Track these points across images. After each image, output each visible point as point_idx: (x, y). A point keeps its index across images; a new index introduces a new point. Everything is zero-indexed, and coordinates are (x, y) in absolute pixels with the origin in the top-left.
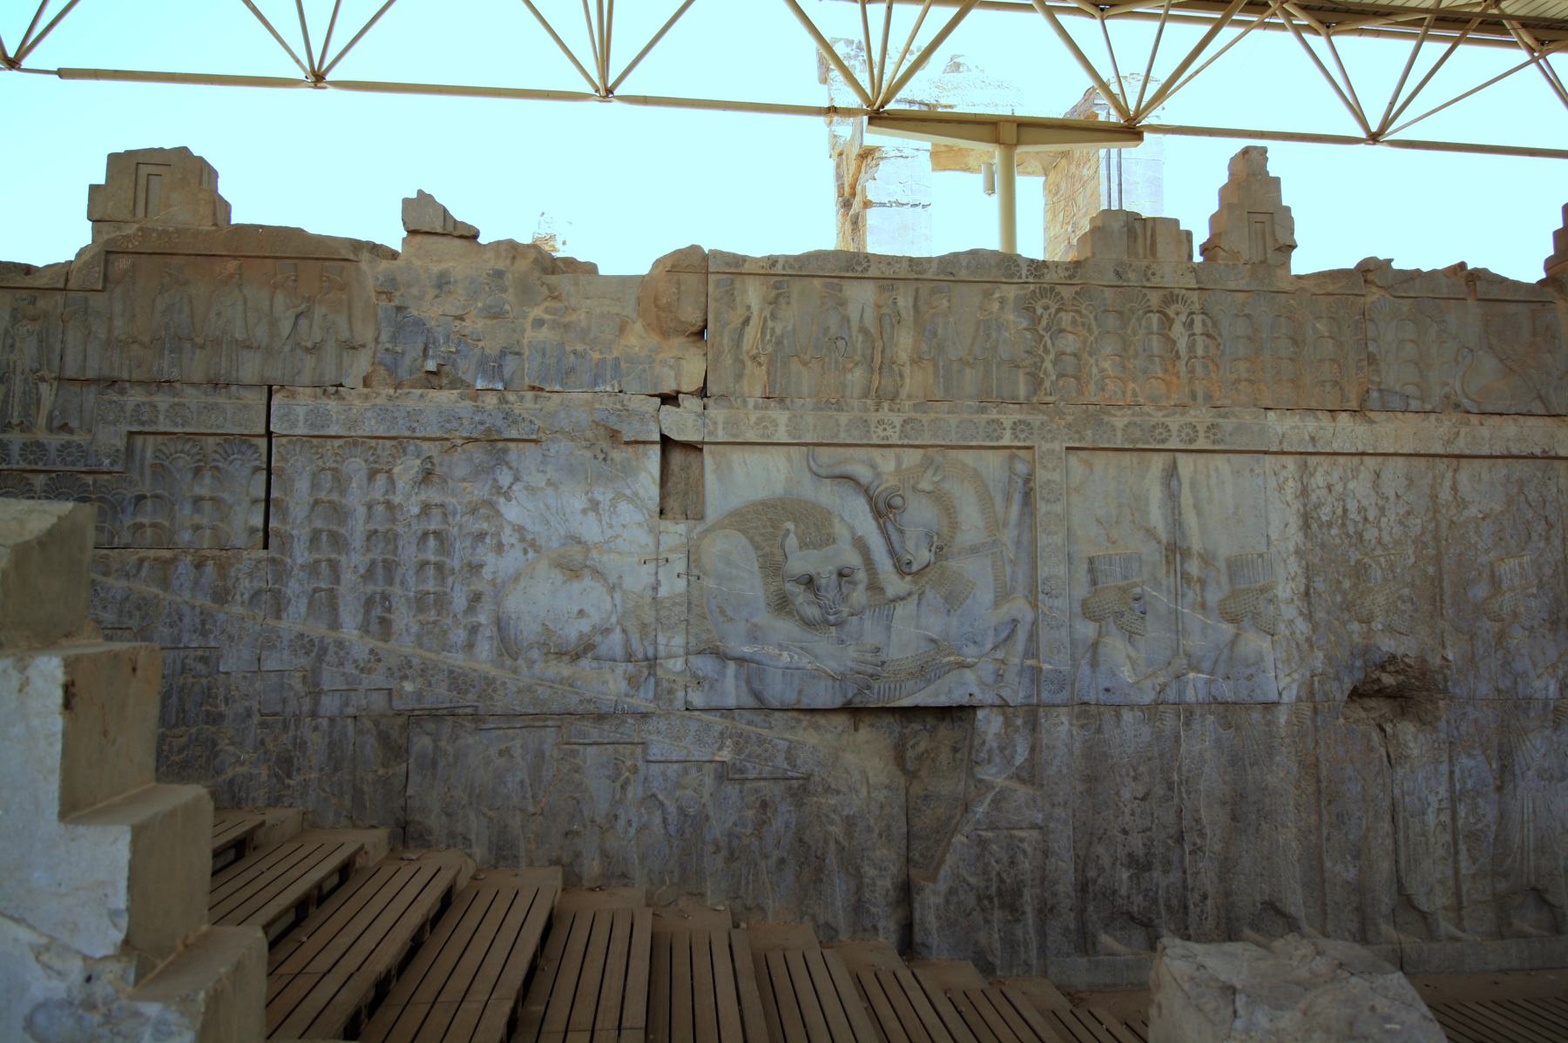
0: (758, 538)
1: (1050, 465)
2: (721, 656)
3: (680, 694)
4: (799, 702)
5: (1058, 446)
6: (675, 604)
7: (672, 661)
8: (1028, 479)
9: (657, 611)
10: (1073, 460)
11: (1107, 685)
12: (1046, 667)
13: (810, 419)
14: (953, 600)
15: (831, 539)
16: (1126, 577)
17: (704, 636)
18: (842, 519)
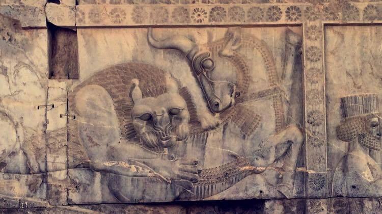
0: (114, 91)
1: (313, 36)
2: (90, 168)
3: (64, 195)
4: (143, 198)
5: (318, 23)
6: (58, 135)
7: (58, 173)
8: (299, 46)
9: (46, 140)
10: (330, 33)
11: (353, 183)
12: (310, 172)
13: (148, 9)
14: (246, 130)
15: (164, 90)
16: (366, 111)
17: (79, 156)
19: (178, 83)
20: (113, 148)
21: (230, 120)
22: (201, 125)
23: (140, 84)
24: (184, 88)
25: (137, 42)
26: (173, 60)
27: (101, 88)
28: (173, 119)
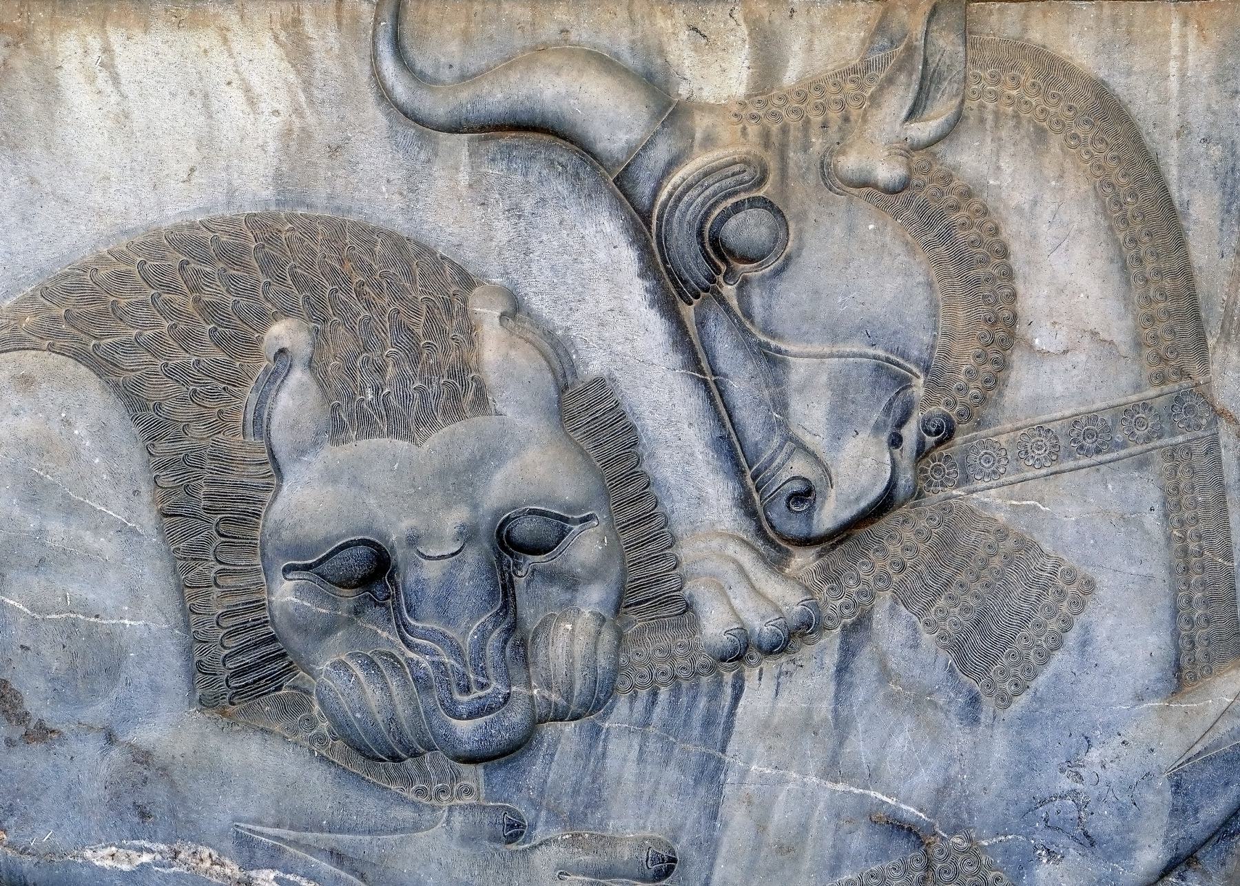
14: (989, 657)
15: (464, 392)
18: (515, 309)
19: (558, 354)
20: (143, 757)
21: (884, 601)
22: (695, 625)
23: (316, 346)
24: (599, 382)
25: (307, 85)
26: (528, 205)
27: (71, 367)
28: (520, 582)
